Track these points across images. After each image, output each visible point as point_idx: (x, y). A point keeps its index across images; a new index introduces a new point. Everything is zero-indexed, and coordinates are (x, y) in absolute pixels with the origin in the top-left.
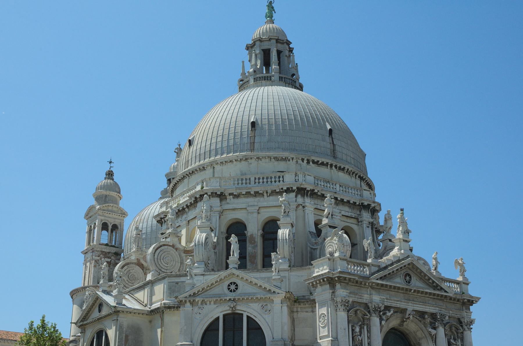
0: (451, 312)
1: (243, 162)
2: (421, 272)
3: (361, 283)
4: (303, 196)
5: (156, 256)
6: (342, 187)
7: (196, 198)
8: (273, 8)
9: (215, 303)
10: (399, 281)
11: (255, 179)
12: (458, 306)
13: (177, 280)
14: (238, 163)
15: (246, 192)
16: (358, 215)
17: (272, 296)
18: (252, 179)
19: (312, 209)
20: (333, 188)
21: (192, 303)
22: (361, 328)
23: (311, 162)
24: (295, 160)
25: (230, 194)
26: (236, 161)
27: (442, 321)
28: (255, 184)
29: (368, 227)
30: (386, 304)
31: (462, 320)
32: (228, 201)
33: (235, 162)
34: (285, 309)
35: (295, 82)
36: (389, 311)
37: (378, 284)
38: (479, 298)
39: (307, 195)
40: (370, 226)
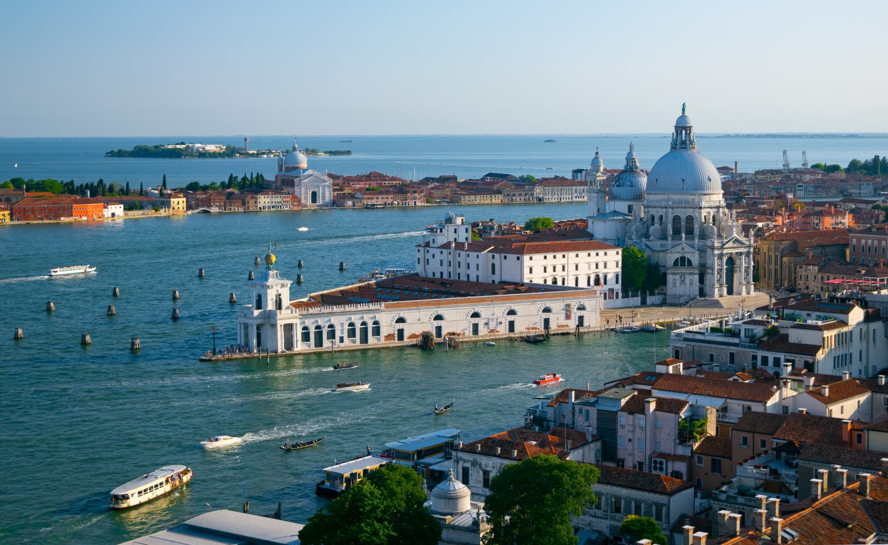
21: (671, 253)
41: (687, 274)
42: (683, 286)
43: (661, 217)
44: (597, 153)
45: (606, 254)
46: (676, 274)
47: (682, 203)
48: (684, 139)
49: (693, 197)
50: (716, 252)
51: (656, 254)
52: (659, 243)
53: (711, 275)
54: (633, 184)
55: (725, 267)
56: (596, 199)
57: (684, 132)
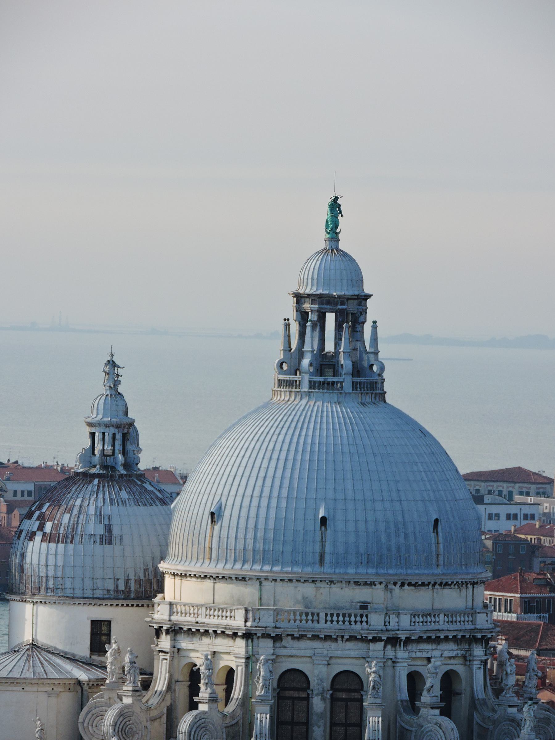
1: (307, 584)
4: (394, 645)
6: (448, 617)
11: (326, 615)
14: (299, 584)
15: (313, 635)
16: (466, 651)
18: (322, 615)
20: (434, 622)
23: (406, 586)
25: (288, 635)
28: (326, 623)
29: (479, 668)
32: (284, 643)
33: (295, 583)
40: (482, 666)
54: (116, 531)
57: (330, 318)
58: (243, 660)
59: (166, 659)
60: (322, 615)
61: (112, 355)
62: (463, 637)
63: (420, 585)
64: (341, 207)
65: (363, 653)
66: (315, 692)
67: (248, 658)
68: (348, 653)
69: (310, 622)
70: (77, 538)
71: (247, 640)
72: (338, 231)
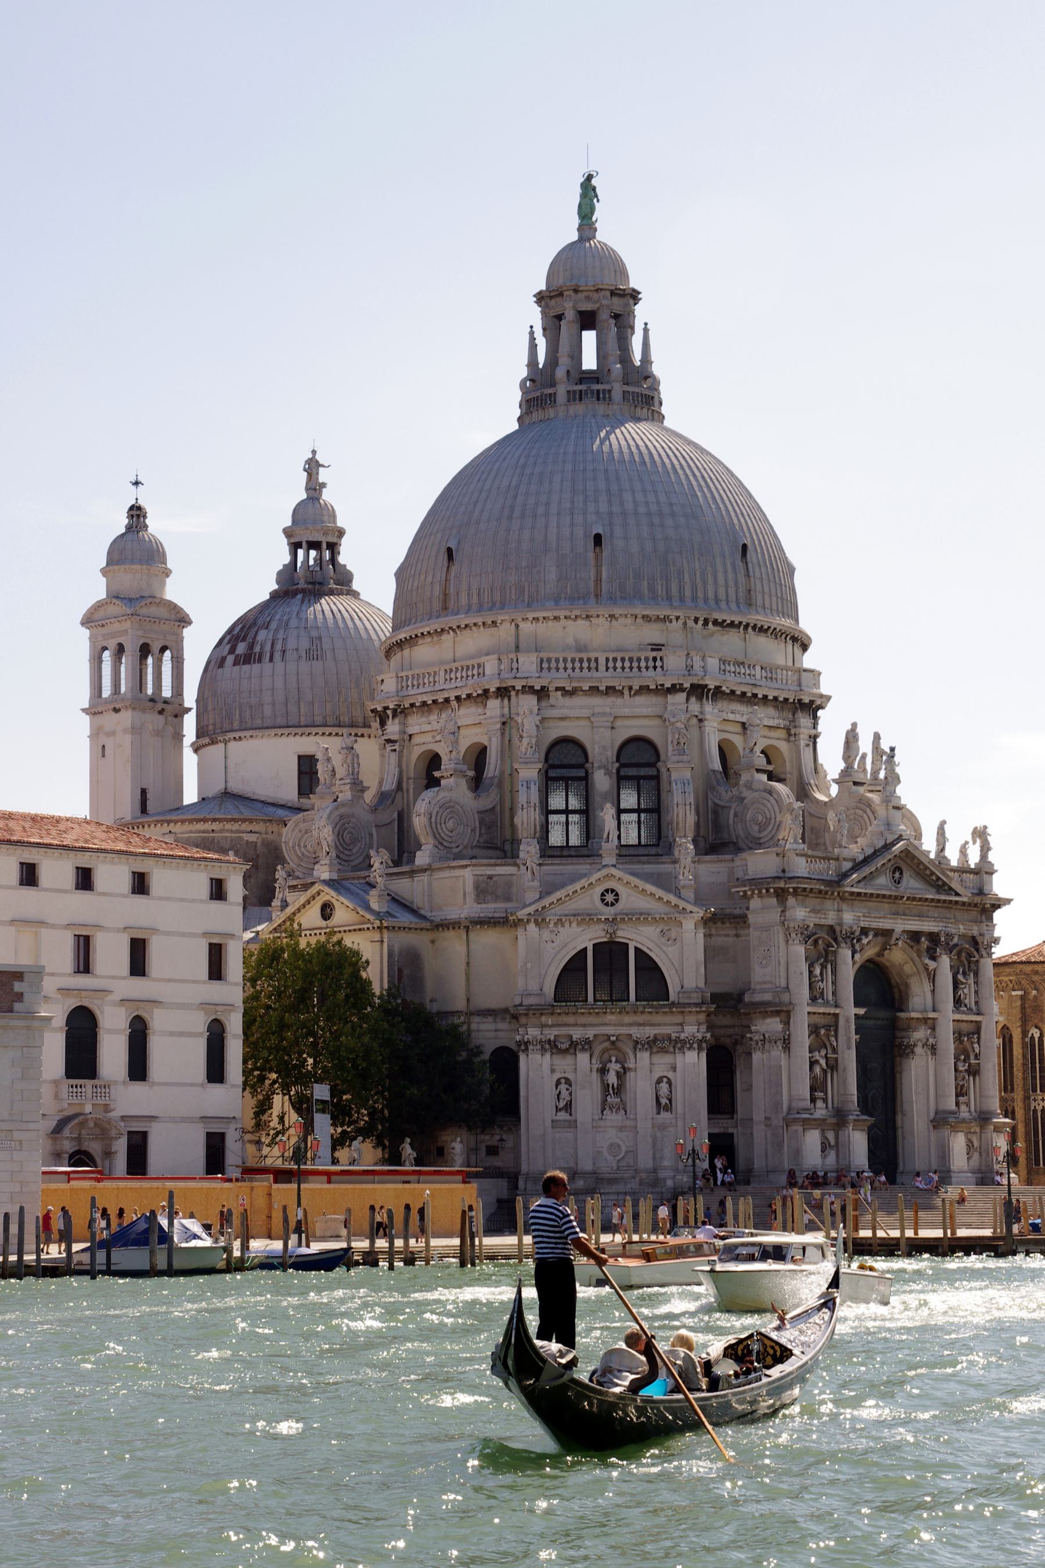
0: (961, 927)
1: (580, 622)
2: (920, 863)
3: (826, 893)
4: (700, 698)
5: (433, 820)
7: (486, 691)
8: (594, 189)
9: (579, 924)
10: (883, 883)
11: (607, 660)
12: (974, 913)
13: (489, 873)
14: (570, 623)
17: (680, 917)
18: (602, 661)
19: (715, 724)
21: (540, 922)
22: (823, 967)
23: (710, 624)
24: (681, 622)
26: (565, 617)
27: (948, 944)
29: (808, 745)
30: (862, 924)
31: (979, 940)
32: (552, 700)
33: (563, 622)
34: (701, 936)
35: (653, 398)
36: (867, 936)
37: (852, 894)
38: (1008, 901)
39: (707, 698)
41: (637, 1043)
42: (613, 1118)
43: (479, 757)
44: (136, 513)
45: (140, 885)
46: (574, 1047)
47: (593, 664)
48: (589, 338)
49: (653, 633)
50: (800, 913)
51: (454, 944)
52: (466, 876)
53: (777, 1052)
54: (326, 644)
55: (853, 1011)
56: (128, 738)
58: (498, 726)
59: (395, 750)
60: (602, 661)
61: (314, 452)
62: (786, 700)
63: (729, 625)
64: (598, 190)
65: (658, 710)
66: (596, 765)
67: (504, 723)
68: (638, 711)
69: (585, 671)
70: (277, 656)
71: (502, 700)
72: (594, 219)
